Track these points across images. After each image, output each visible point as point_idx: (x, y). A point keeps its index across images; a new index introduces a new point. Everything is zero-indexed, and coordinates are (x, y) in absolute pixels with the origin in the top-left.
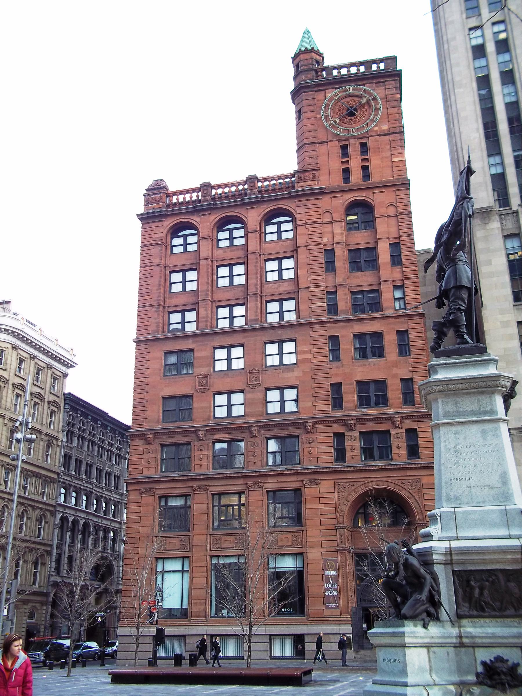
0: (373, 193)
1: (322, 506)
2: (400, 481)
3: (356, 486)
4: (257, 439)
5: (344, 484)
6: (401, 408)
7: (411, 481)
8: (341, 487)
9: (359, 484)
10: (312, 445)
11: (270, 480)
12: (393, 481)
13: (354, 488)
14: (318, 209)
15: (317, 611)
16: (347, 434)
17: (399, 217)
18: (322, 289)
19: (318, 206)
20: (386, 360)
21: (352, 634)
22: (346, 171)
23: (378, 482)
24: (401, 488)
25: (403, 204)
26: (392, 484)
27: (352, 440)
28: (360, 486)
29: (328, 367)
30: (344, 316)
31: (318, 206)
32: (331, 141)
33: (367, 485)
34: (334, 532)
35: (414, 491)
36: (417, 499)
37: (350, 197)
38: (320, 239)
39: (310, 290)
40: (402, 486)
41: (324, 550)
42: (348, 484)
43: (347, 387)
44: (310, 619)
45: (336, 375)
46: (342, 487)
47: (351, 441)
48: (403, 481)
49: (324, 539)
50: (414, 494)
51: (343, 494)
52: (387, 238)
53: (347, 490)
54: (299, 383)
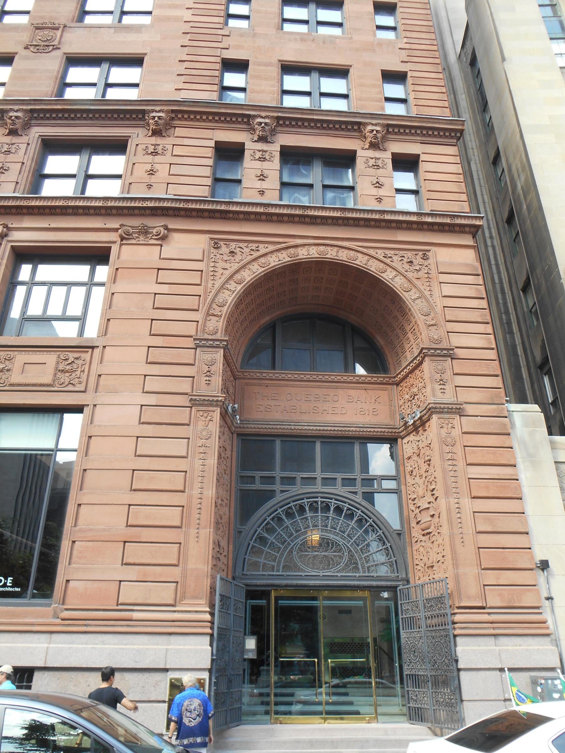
1: (165, 289)
2: (380, 252)
3: (263, 251)
4: (15, 140)
5: (233, 245)
7: (409, 254)
8: (224, 250)
9: (271, 248)
10: (158, 158)
11: (28, 222)
12: (365, 250)
13: (256, 254)
15: (96, 584)
16: (251, 146)
21: (210, 671)
23: (322, 248)
24: (382, 266)
26: (360, 255)
27: (262, 159)
28: (272, 252)
33: (292, 251)
34: (187, 356)
35: (416, 275)
36: (427, 293)
40: (388, 261)
41: (152, 399)
42: (241, 245)
43: (260, 68)
44: (66, 614)
45: (238, 47)
46: (227, 251)
47: (259, 159)
48: (387, 252)
49: (156, 370)
50: (418, 283)
51: (227, 265)
53: (238, 257)
54: (149, 52)
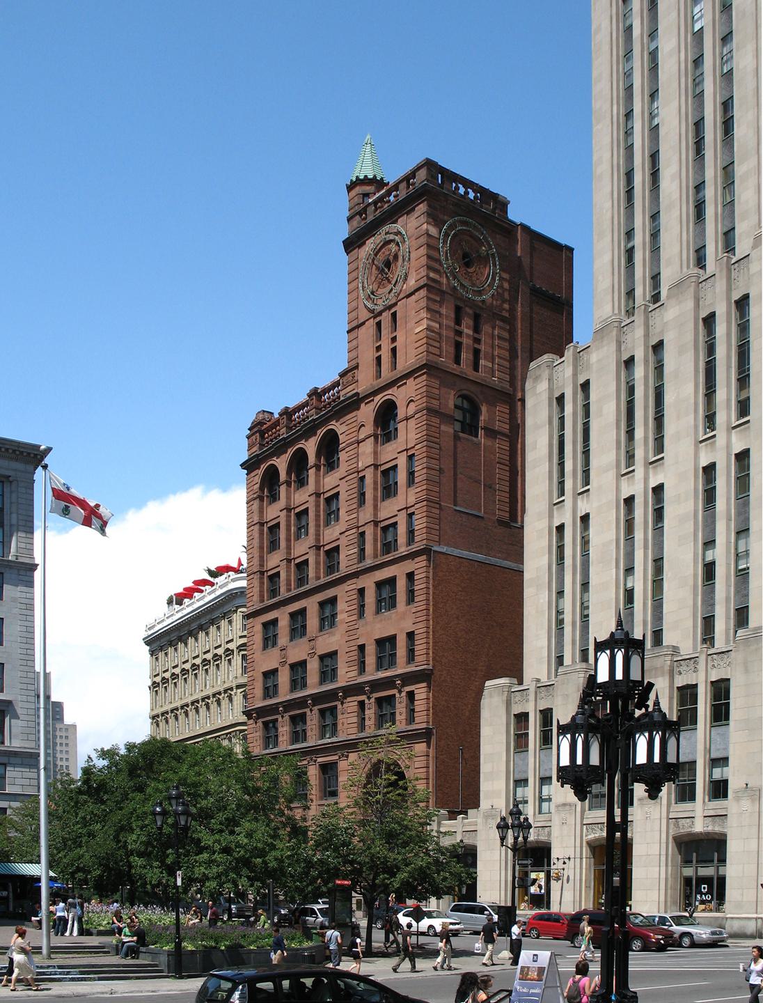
0: (398, 387)
6: (405, 668)
14: (354, 424)
17: (416, 416)
18: (354, 531)
19: (355, 419)
20: (397, 612)
22: (379, 359)
25: (419, 397)
29: (356, 627)
30: (369, 562)
31: (355, 419)
32: (368, 320)
37: (379, 399)
38: (355, 465)
39: (347, 533)
52: (404, 450)
